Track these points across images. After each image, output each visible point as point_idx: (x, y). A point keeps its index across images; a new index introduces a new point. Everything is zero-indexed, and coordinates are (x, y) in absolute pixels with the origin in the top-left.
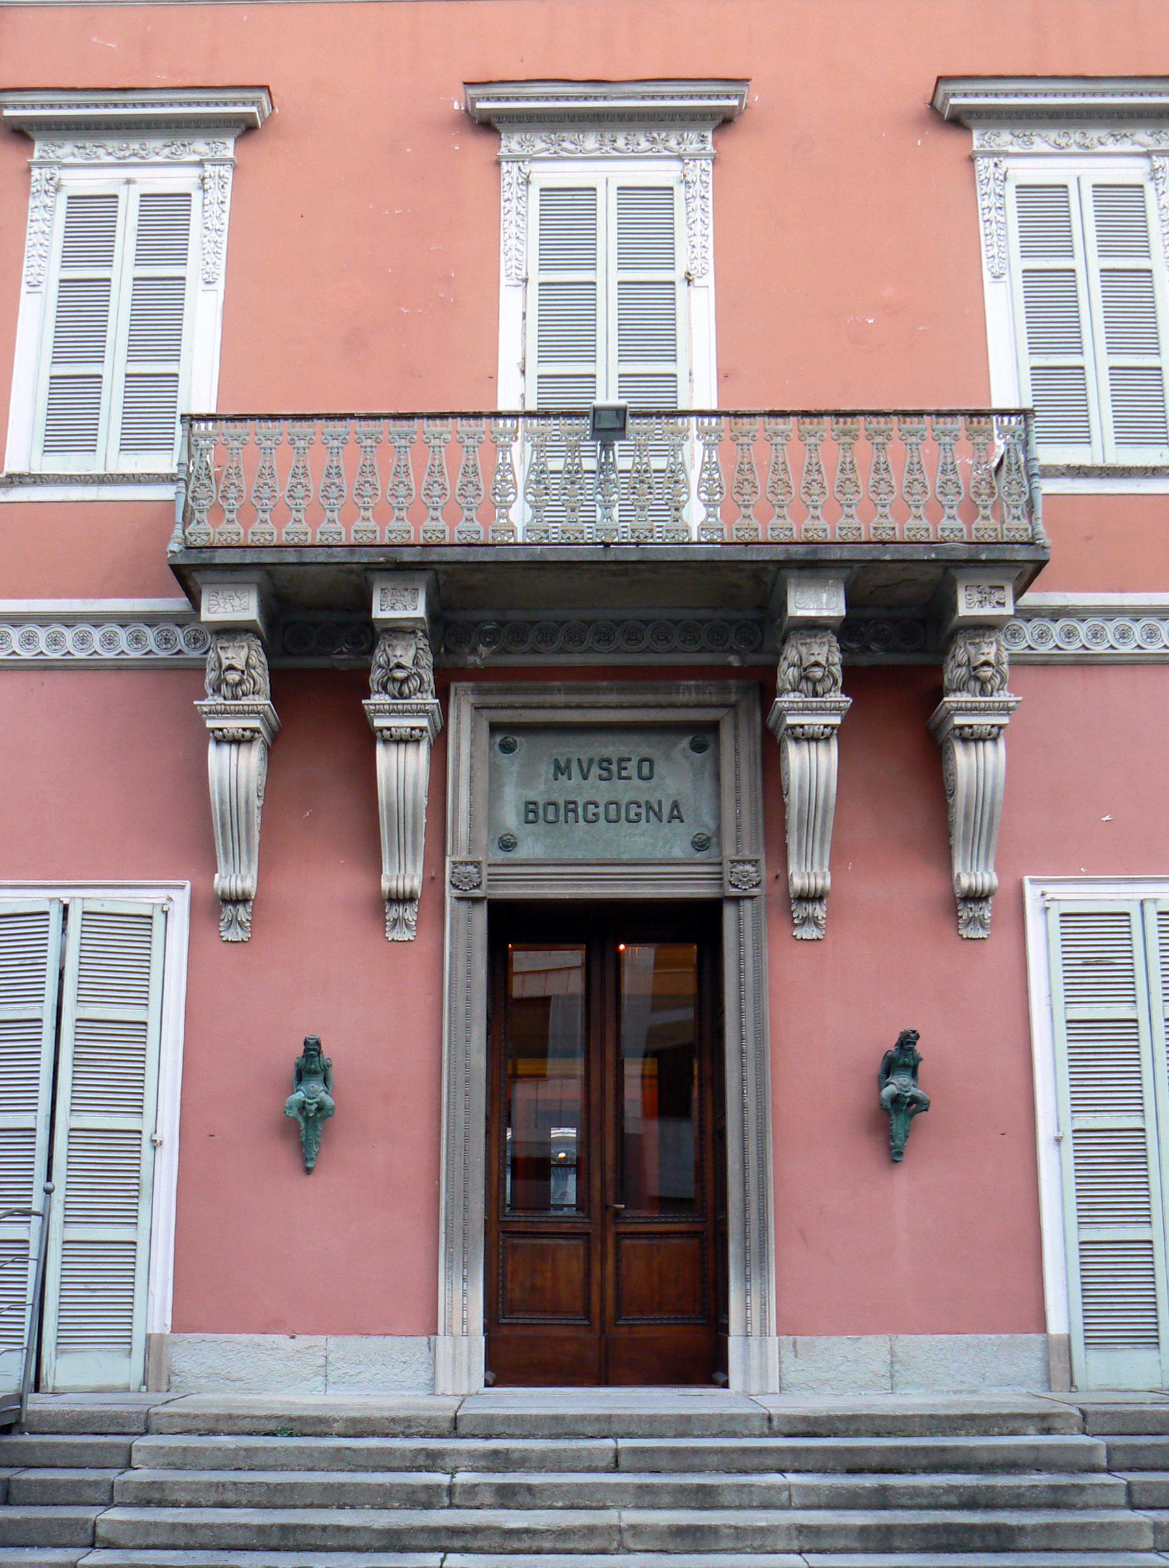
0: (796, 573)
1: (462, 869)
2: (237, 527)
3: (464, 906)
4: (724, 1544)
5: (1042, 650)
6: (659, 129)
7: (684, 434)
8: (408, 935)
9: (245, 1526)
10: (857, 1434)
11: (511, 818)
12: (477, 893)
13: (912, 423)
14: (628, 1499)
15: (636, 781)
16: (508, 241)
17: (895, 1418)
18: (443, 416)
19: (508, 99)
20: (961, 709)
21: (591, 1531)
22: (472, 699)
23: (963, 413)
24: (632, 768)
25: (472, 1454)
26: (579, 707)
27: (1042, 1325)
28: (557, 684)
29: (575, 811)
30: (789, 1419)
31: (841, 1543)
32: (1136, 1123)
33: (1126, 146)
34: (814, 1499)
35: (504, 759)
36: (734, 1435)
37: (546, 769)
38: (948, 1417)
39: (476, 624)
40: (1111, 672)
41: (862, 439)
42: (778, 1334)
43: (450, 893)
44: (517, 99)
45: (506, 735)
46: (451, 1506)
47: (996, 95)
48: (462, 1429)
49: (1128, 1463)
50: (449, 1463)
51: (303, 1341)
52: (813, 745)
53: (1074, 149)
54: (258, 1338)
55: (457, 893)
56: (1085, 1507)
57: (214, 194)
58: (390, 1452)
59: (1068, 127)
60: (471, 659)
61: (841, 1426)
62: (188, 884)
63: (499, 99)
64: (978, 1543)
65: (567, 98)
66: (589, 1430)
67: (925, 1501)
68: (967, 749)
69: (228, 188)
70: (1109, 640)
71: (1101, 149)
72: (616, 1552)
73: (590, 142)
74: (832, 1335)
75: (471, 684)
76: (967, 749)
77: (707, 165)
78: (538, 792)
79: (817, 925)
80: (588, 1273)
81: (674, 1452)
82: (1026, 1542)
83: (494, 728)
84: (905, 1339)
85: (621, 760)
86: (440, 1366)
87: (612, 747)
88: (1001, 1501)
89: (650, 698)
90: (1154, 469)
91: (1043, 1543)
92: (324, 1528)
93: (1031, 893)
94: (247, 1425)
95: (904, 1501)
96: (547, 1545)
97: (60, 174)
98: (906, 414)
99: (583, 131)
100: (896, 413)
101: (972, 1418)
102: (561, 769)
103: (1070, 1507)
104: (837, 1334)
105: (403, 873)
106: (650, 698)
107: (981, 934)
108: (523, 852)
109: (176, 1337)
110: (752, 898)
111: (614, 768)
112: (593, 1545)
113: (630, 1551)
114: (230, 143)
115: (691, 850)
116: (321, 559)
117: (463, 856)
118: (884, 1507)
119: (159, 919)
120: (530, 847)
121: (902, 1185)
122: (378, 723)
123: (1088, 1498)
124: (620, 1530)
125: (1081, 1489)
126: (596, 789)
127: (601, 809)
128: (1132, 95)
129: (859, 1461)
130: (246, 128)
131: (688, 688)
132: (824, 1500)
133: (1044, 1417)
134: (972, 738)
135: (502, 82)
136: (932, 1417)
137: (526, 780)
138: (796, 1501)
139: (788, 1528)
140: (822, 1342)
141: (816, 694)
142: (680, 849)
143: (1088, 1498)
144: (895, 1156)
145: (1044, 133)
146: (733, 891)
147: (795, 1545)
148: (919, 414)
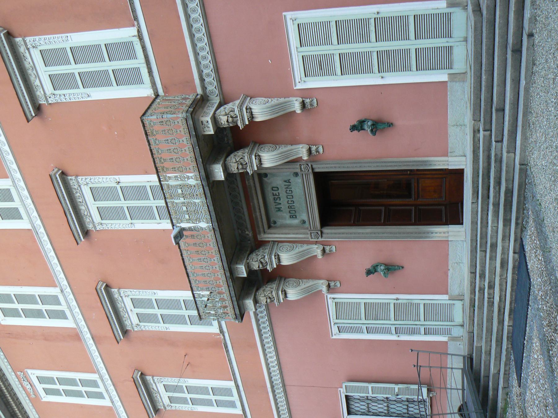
0: (211, 179)
1: (313, 237)
2: (228, 308)
3: (324, 235)
4: (506, 257)
5: (215, 84)
6: (72, 191)
7: (168, 186)
8: (334, 247)
9: (496, 348)
10: (478, 181)
11: (295, 222)
12: (319, 233)
13: (155, 151)
14: (493, 262)
15: (279, 191)
16: (121, 228)
17: (473, 171)
18: (185, 267)
19: (78, 233)
20: (241, 106)
21: (501, 285)
22: (262, 235)
23: (147, 138)
24: (276, 192)
25: (480, 281)
26: (260, 209)
27: (445, 83)
28: (254, 215)
29: (291, 206)
30: (473, 198)
31: (508, 231)
32: (375, 54)
33: (27, 55)
34: (496, 221)
35: (278, 223)
36: (477, 212)
37: (279, 213)
38: (474, 158)
39: (240, 235)
40: (218, 60)
41: (156, 137)
42: (447, 156)
43: (320, 239)
44: (77, 230)
45: (271, 224)
46: (493, 298)
47: (27, 102)
48: (474, 271)
49: (489, 125)
50: (482, 286)
51: (450, 267)
52: (262, 160)
53: (35, 72)
54: (449, 278)
55: (320, 238)
56: (502, 154)
57: (129, 293)
58: (479, 298)
59: (27, 74)
60: (250, 235)
61: (475, 185)
63: (79, 235)
64: (510, 198)
65: (73, 219)
66: (475, 244)
67: (498, 194)
68: (256, 118)
69: (126, 290)
70: (207, 61)
71: (31, 63)
72: (507, 280)
73: (82, 208)
74: (447, 133)
75: (258, 237)
76: (256, 118)
77: (80, 178)
78: (288, 216)
79: (312, 101)
80: (428, 178)
81: (481, 238)
82: (510, 186)
83: (269, 227)
84: (449, 122)
85: (274, 195)
86: (456, 239)
87: (270, 198)
88: (499, 175)
89: (254, 192)
90: (142, 48)
91: (511, 182)
92: (497, 334)
93: (299, 86)
94: (472, 314)
95: (497, 200)
96: (504, 293)
97: (134, 325)
98: (152, 154)
99: (80, 210)
100: (153, 157)
101: (474, 151)
102: (279, 210)
103: (501, 158)
104: (448, 140)
105: (317, 251)
106: (254, 192)
107: (315, 101)
108: (306, 218)
109: (449, 293)
110: (312, 166)
111: (276, 197)
112: (504, 284)
113: (507, 277)
114: (113, 290)
115: (298, 177)
116: (233, 292)
117: (309, 236)
118: (499, 204)
119: (336, 300)
120: (304, 217)
121: (399, 122)
122: (275, 266)
123: (499, 153)
124: (501, 279)
125: (496, 155)
126: (284, 201)
127: (290, 200)
128: (10, 60)
129: (486, 195)
130: (108, 287)
131: (249, 183)
132: (496, 219)
133: (474, 132)
134: (252, 116)
135: (74, 237)
136: (473, 162)
137: (285, 218)
138: (496, 225)
139: (502, 243)
140: (450, 145)
141: (247, 164)
142: (299, 180)
143: (499, 153)
144: (390, 125)
145: (33, 82)
146: (310, 171)
147: (507, 241)
148: (151, 150)
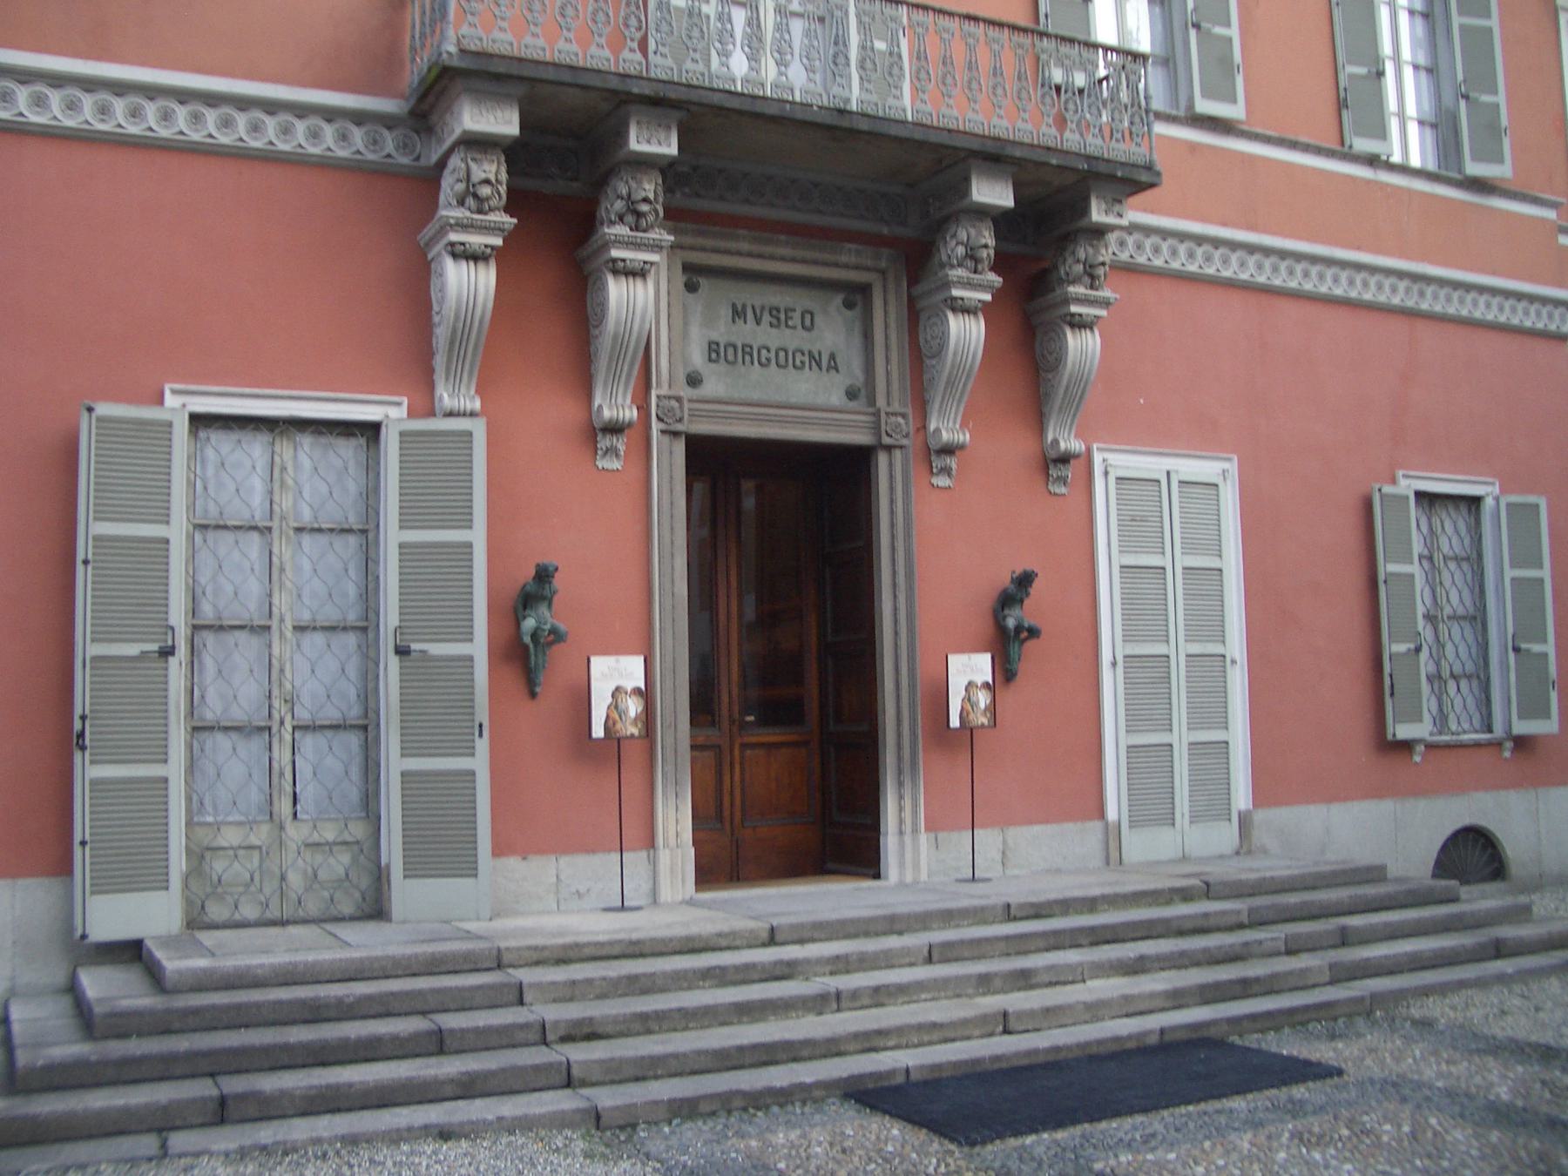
1: (666, 402)
3: (666, 439)
8: (616, 464)
11: (697, 358)
12: (679, 427)
27: (1101, 813)
37: (726, 312)
43: (656, 426)
48: (778, 938)
55: (662, 426)
62: (405, 400)
78: (722, 331)
83: (688, 268)
93: (1098, 458)
102: (738, 313)
105: (615, 405)
107: (1063, 490)
110: (901, 447)
111: (782, 317)
117: (664, 391)
120: (714, 386)
126: (772, 337)
127: (773, 355)
134: (1080, 324)
142: (837, 398)
